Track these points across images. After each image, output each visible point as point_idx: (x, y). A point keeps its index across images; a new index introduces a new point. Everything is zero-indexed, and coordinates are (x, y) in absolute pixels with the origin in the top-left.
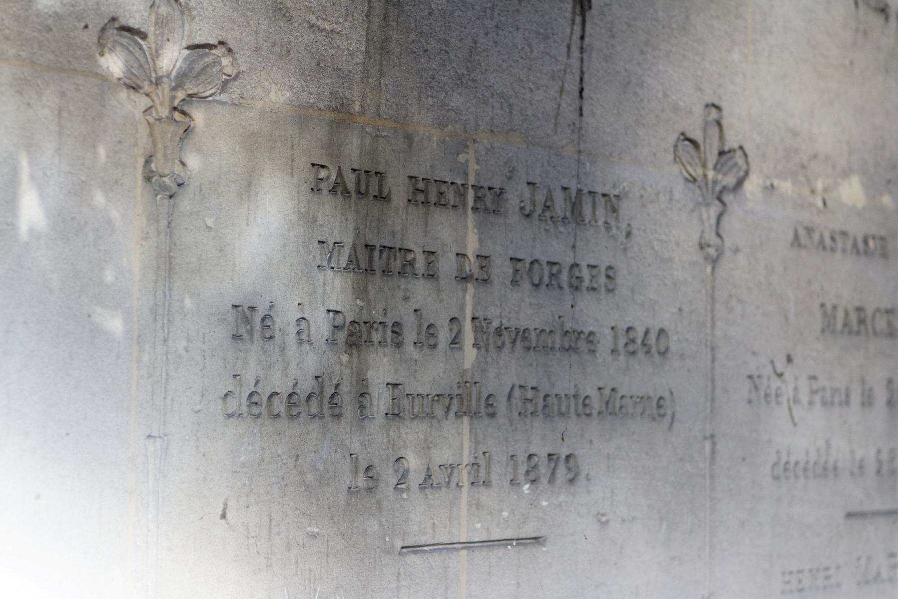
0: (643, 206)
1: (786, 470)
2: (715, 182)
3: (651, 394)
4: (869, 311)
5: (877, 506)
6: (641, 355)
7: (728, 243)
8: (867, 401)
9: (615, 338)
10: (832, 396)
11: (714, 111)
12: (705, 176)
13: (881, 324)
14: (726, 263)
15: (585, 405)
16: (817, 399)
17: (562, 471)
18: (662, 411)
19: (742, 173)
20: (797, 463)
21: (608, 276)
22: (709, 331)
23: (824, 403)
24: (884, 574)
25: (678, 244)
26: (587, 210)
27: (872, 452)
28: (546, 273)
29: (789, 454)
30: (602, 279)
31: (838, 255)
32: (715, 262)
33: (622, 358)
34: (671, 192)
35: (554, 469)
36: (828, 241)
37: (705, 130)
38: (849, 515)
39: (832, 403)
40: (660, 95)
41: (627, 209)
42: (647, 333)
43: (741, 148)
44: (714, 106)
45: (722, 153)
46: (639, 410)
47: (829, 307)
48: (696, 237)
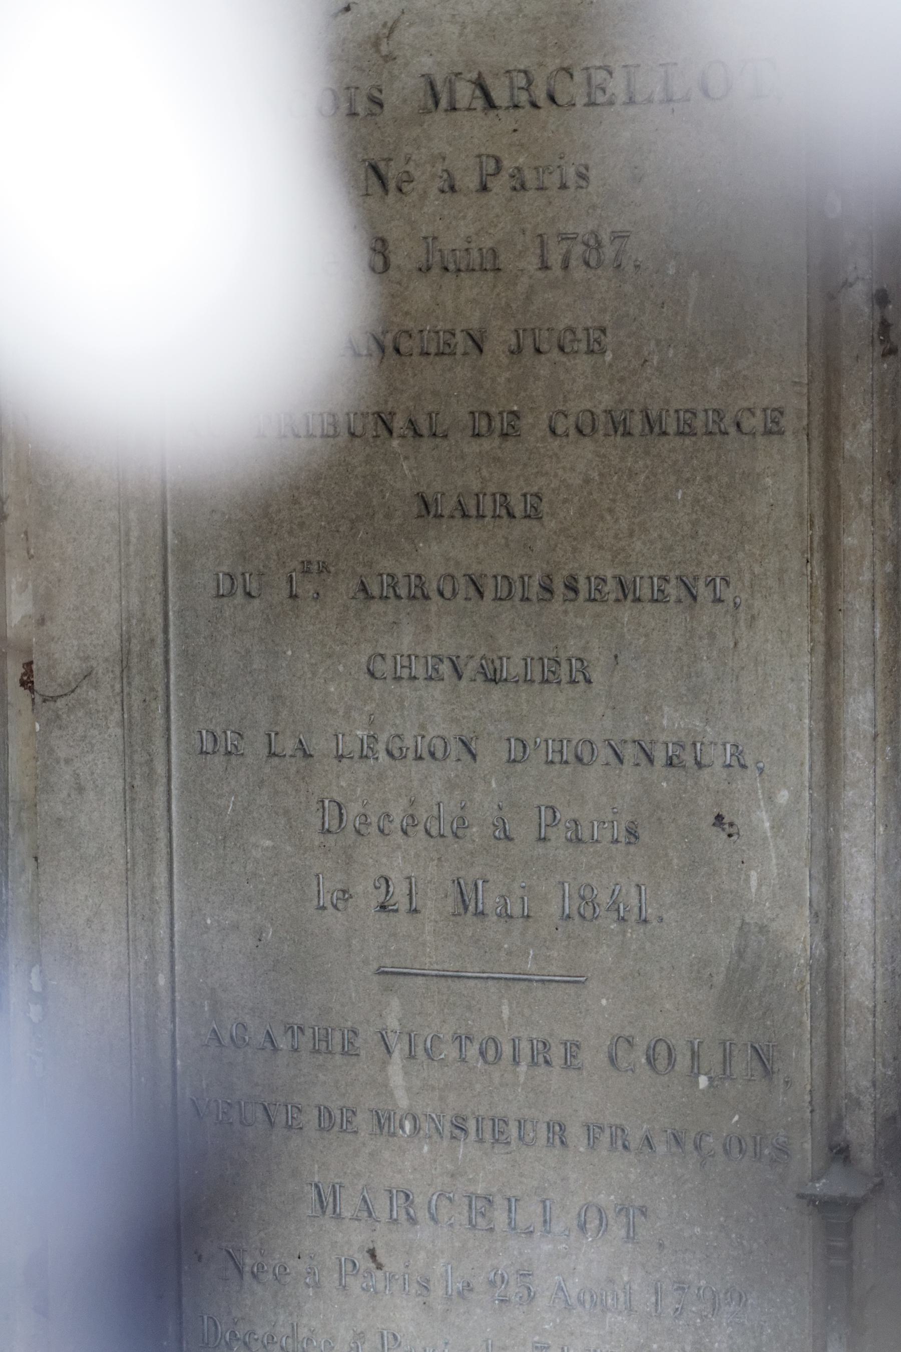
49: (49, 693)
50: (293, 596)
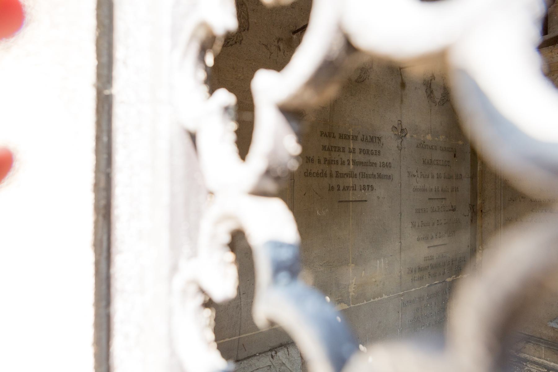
0: (386, 139)
1: (416, 190)
2: (400, 135)
3: (388, 175)
4: (433, 160)
5: (435, 197)
6: (386, 167)
7: (403, 146)
8: (433, 177)
9: (380, 164)
10: (425, 176)
11: (400, 121)
12: (398, 134)
13: (435, 163)
14: (403, 150)
15: (374, 176)
16: (422, 176)
17: (370, 188)
18: (390, 178)
19: (406, 133)
20: (418, 189)
21: (379, 152)
22: (400, 163)
23: (424, 177)
24: (437, 210)
25: (393, 147)
26: (374, 140)
27: (434, 187)
28: (366, 151)
29: (416, 187)
30: (378, 153)
31: (426, 149)
32: (400, 150)
33: (382, 167)
34: (391, 137)
35: (369, 187)
36: (424, 147)
37: (398, 125)
38: (429, 199)
39: (425, 177)
40: (389, 118)
41: (383, 140)
42: (387, 163)
43: (406, 129)
44: (400, 120)
45: (402, 130)
46: (385, 177)
47: (424, 159)
48: (397, 145)
49: (484, 212)
50: (520, 201)
